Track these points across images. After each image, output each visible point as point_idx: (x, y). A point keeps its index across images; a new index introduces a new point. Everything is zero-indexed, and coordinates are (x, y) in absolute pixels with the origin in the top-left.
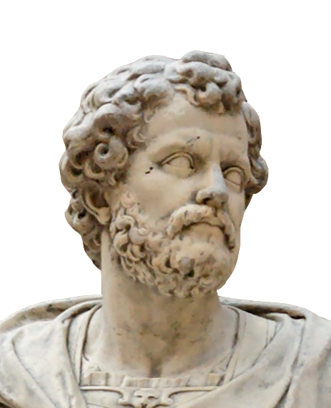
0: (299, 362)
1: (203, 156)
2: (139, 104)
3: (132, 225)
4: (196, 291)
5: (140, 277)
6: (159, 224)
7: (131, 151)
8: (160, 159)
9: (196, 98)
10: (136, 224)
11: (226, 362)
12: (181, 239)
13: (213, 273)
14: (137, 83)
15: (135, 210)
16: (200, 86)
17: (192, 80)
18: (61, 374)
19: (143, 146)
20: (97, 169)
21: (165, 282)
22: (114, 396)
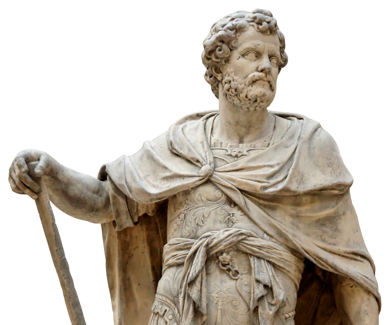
0: (301, 137)
1: (261, 52)
2: (234, 31)
3: (232, 81)
4: (258, 108)
5: (235, 102)
6: (243, 80)
7: (231, 50)
8: (243, 53)
9: (258, 28)
10: (233, 80)
11: (270, 137)
12: (252, 86)
13: (265, 101)
14: (234, 22)
15: (233, 75)
16: (260, 23)
17: (256, 21)
18: (202, 142)
19: (236, 48)
20: (217, 58)
21: (245, 104)
22: (224, 151)
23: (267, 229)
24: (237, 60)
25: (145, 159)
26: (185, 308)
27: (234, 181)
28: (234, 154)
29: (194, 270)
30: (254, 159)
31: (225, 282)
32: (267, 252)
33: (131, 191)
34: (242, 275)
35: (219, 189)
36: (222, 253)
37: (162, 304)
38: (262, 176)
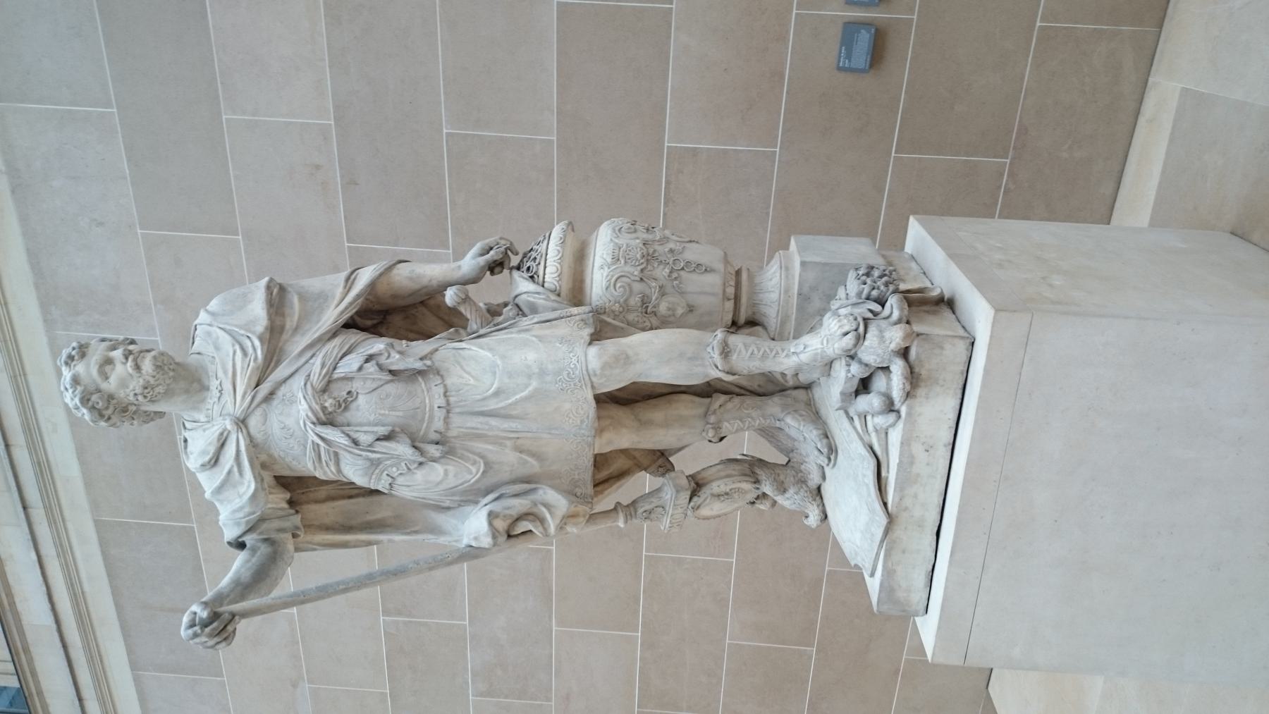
4: (171, 367)
7: (100, 391)
9: (78, 360)
10: (134, 390)
15: (128, 391)
22: (215, 406)
23: (303, 360)
24: (111, 385)
25: (221, 497)
26: (384, 451)
27: (245, 393)
28: (218, 395)
29: (342, 439)
30: (225, 372)
31: (359, 406)
32: (330, 359)
33: (254, 513)
34: (352, 387)
35: (254, 410)
36: (324, 409)
37: (379, 480)
38: (243, 361)
